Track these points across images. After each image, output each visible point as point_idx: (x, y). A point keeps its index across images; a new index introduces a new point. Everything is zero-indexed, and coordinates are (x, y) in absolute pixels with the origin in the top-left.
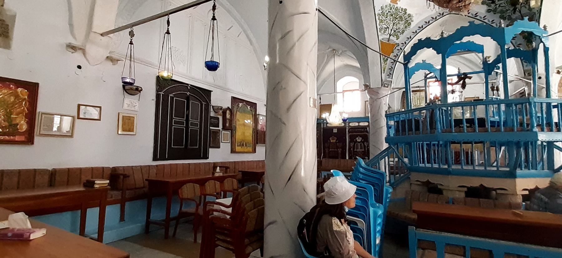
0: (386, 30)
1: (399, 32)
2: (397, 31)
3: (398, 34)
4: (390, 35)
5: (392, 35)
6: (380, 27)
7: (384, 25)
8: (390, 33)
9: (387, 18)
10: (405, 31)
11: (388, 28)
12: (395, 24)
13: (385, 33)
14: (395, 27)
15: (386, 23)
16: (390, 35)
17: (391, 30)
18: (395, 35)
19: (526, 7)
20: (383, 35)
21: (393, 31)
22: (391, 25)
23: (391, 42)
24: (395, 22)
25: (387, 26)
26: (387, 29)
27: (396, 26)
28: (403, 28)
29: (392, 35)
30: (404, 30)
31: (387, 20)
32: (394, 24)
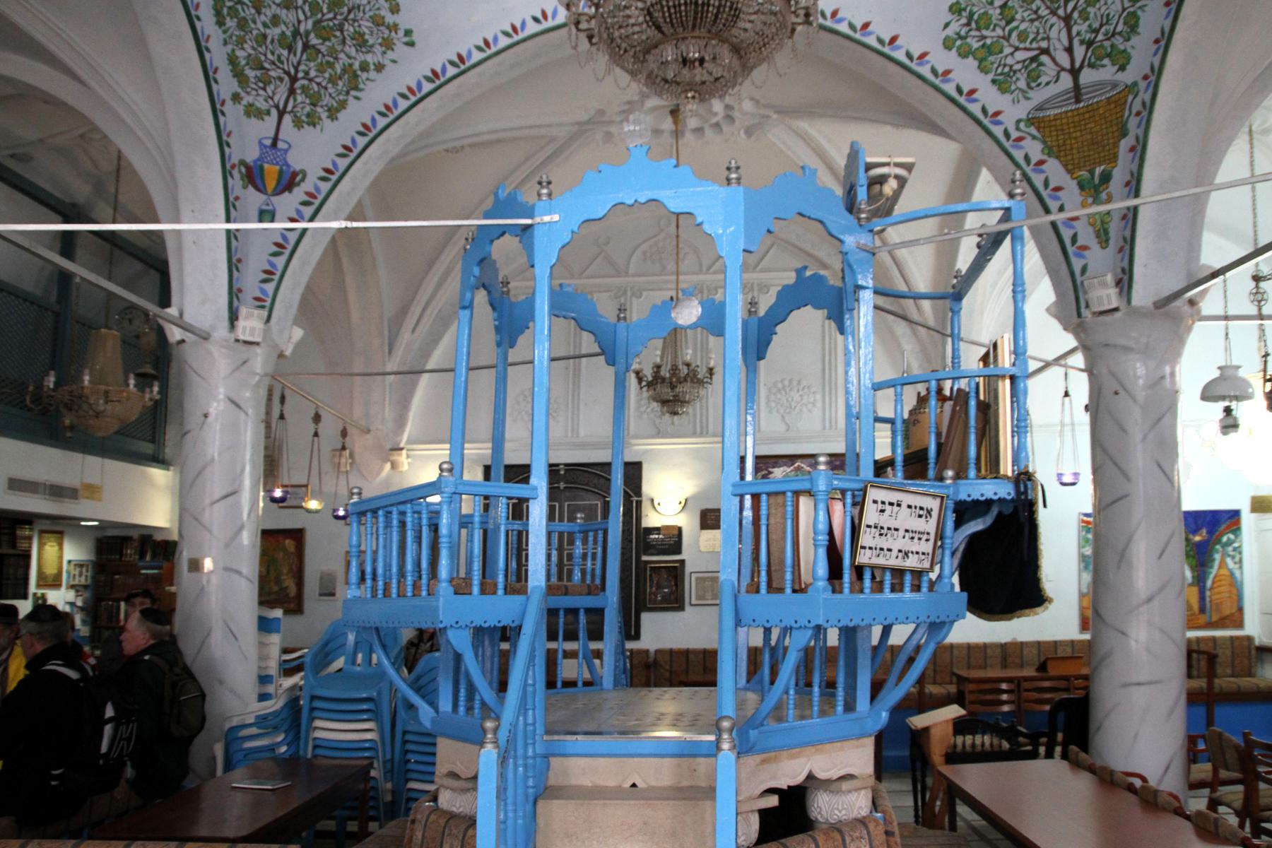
0: (1041, 64)
1: (1114, 34)
2: (1100, 37)
3: (1112, 46)
4: (1075, 72)
5: (1082, 67)
6: (991, 76)
7: (1012, 54)
8: (1067, 65)
9: (1013, 19)
10: (1139, 13)
11: (1046, 51)
12: (1076, 15)
13: (1043, 80)
14: (1084, 27)
15: (1024, 41)
16: (1075, 72)
17: (1069, 50)
18: (1101, 59)
20: (1031, 94)
21: (1084, 48)
22: (1053, 34)
23: (1089, 100)
24: (1069, 9)
25: (1034, 45)
26: (1044, 58)
27: (1087, 19)
28: (1124, 10)
29: (1082, 67)
30: (1134, 14)
31: (1017, 27)
32: (1067, 20)
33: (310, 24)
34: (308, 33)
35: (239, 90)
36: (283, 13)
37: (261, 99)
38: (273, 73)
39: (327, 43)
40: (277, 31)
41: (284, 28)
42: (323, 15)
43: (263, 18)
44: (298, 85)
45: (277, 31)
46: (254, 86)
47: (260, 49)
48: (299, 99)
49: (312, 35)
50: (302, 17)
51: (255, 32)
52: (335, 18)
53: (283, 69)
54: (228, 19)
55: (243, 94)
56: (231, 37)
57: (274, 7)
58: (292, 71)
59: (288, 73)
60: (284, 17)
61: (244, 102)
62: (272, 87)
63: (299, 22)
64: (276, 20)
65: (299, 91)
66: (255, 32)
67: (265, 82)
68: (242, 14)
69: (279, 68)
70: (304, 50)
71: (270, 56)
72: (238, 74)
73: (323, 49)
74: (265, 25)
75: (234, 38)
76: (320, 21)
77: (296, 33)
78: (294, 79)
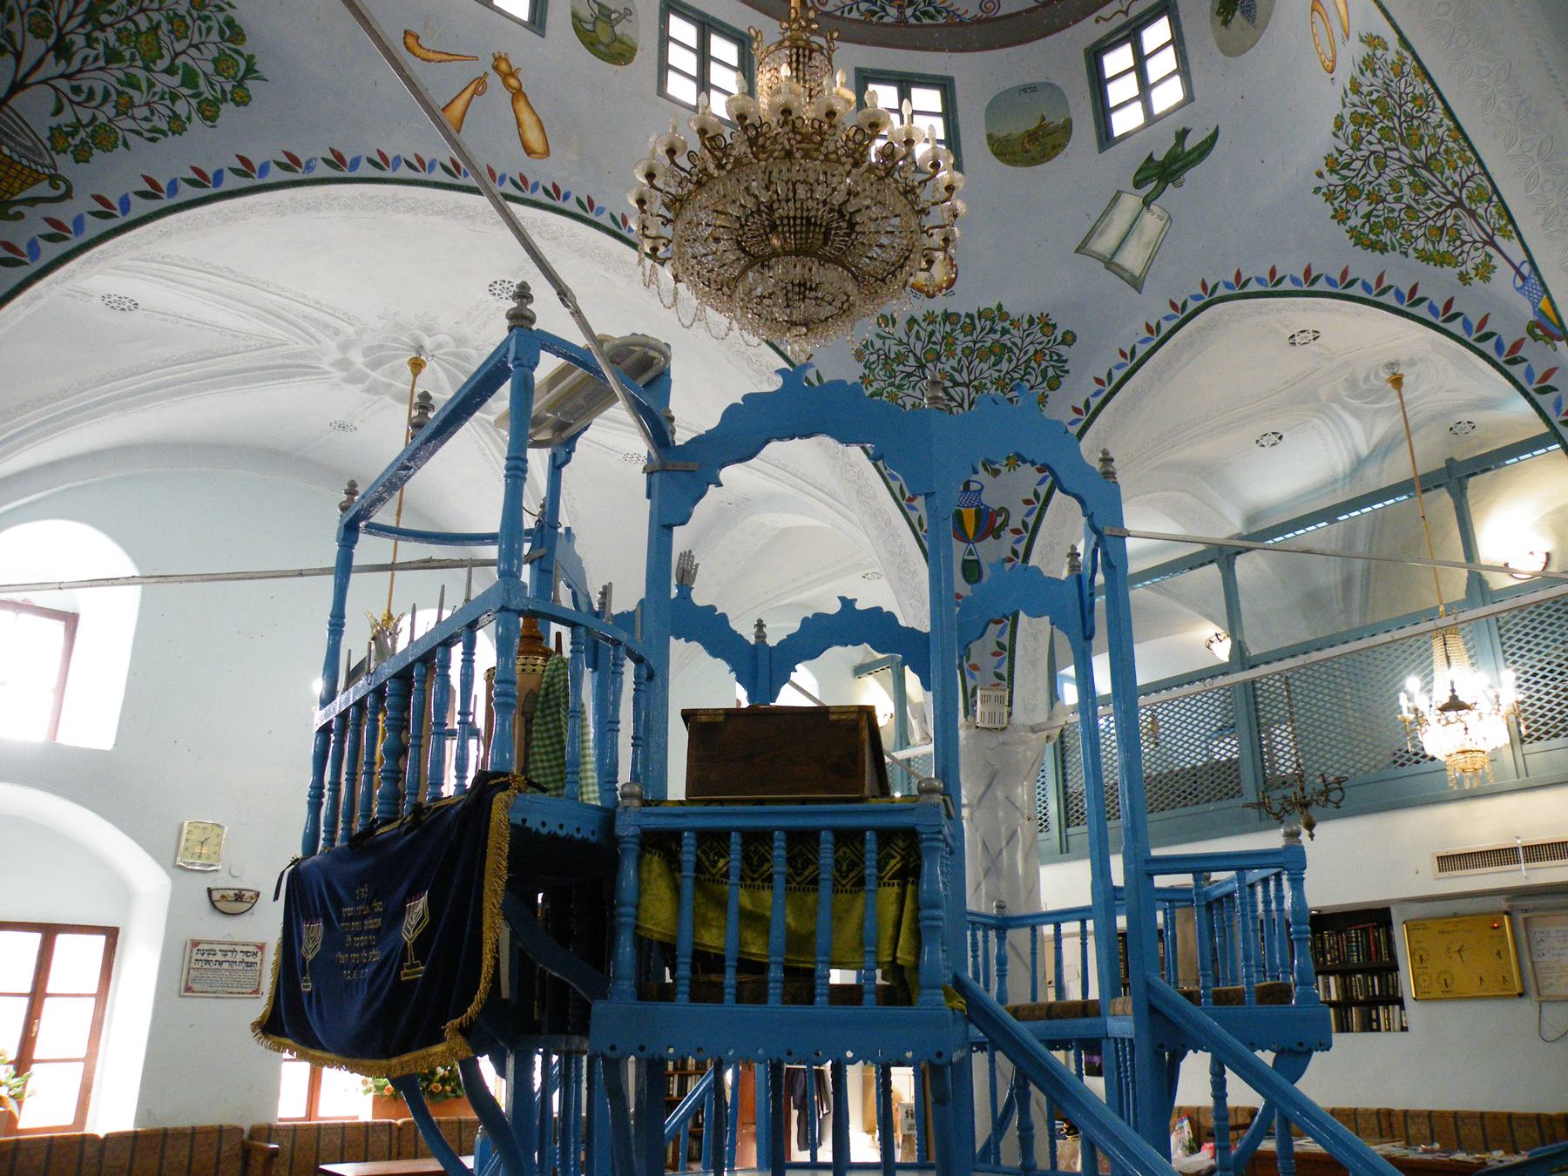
19: (58, 111)
33: (1402, 148)
34: (1413, 157)
35: (1457, 270)
36: (1390, 174)
37: (1473, 254)
38: (1450, 222)
39: (1426, 140)
40: (1406, 189)
41: (1404, 181)
42: (1395, 128)
43: (1390, 198)
44: (1466, 202)
45: (1406, 189)
46: (1458, 251)
47: (1421, 220)
48: (1480, 211)
49: (1416, 152)
50: (1395, 154)
51: (1403, 216)
52: (1399, 118)
53: (1448, 208)
54: (1382, 237)
55: (1463, 268)
56: (1401, 245)
57: (1380, 180)
58: (1450, 198)
59: (1452, 206)
60: (1393, 174)
61: (1472, 273)
62: (1463, 232)
63: (1400, 160)
64: (1395, 185)
65: (1474, 207)
66: (1403, 216)
67: (1456, 237)
68: (1381, 219)
69: (1445, 211)
70: (1431, 172)
71: (1431, 214)
72: (1442, 260)
73: (1431, 150)
74: (1398, 200)
75: (1403, 241)
76: (1401, 134)
77: (1412, 169)
78: (1459, 203)
